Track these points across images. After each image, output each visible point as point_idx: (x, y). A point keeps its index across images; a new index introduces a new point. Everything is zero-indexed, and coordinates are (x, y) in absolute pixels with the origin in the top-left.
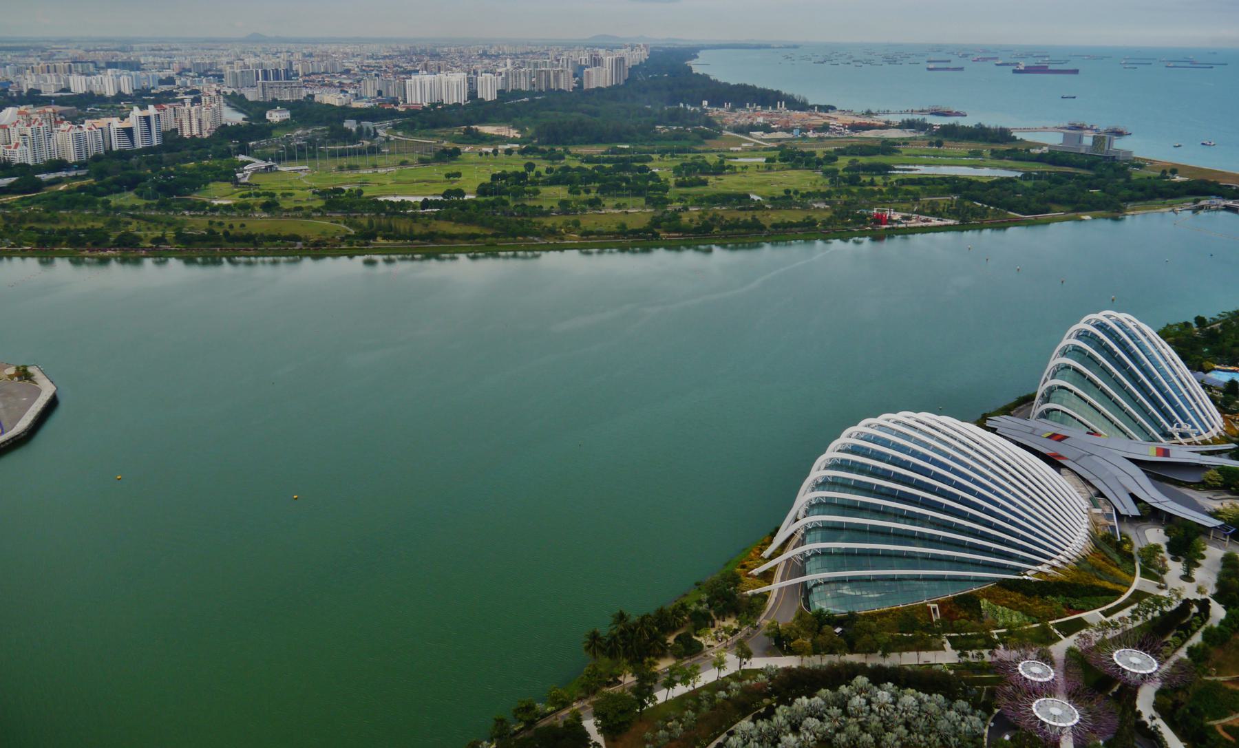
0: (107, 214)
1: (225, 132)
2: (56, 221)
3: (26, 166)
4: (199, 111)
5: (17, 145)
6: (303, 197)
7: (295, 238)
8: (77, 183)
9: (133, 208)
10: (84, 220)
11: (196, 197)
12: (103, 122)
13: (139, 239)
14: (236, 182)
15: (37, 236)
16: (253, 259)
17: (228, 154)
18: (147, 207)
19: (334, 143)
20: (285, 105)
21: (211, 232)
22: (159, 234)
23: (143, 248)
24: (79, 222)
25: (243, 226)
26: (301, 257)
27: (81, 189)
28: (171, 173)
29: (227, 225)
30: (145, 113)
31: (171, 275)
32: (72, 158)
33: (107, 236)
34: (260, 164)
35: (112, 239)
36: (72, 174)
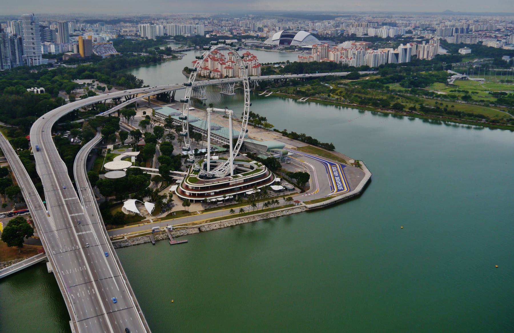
0: (388, 93)
1: (438, 58)
2: (366, 93)
3: (353, 67)
4: (428, 47)
5: (351, 58)
6: (484, 95)
7: (482, 117)
8: (375, 77)
9: (400, 91)
10: (378, 95)
11: (427, 89)
12: (386, 50)
13: (404, 107)
14: (447, 84)
15: (359, 100)
16: (457, 124)
17: (441, 68)
18: (406, 91)
19: (498, 68)
20: (469, 46)
21: (438, 108)
22: (412, 105)
23: (405, 111)
24: (376, 95)
25: (453, 106)
26: (484, 126)
27: (377, 80)
28: (416, 76)
29: (445, 105)
30: (405, 47)
31: (418, 126)
32: (371, 66)
33: (389, 105)
34: (460, 76)
35: (391, 105)
36: (371, 72)
